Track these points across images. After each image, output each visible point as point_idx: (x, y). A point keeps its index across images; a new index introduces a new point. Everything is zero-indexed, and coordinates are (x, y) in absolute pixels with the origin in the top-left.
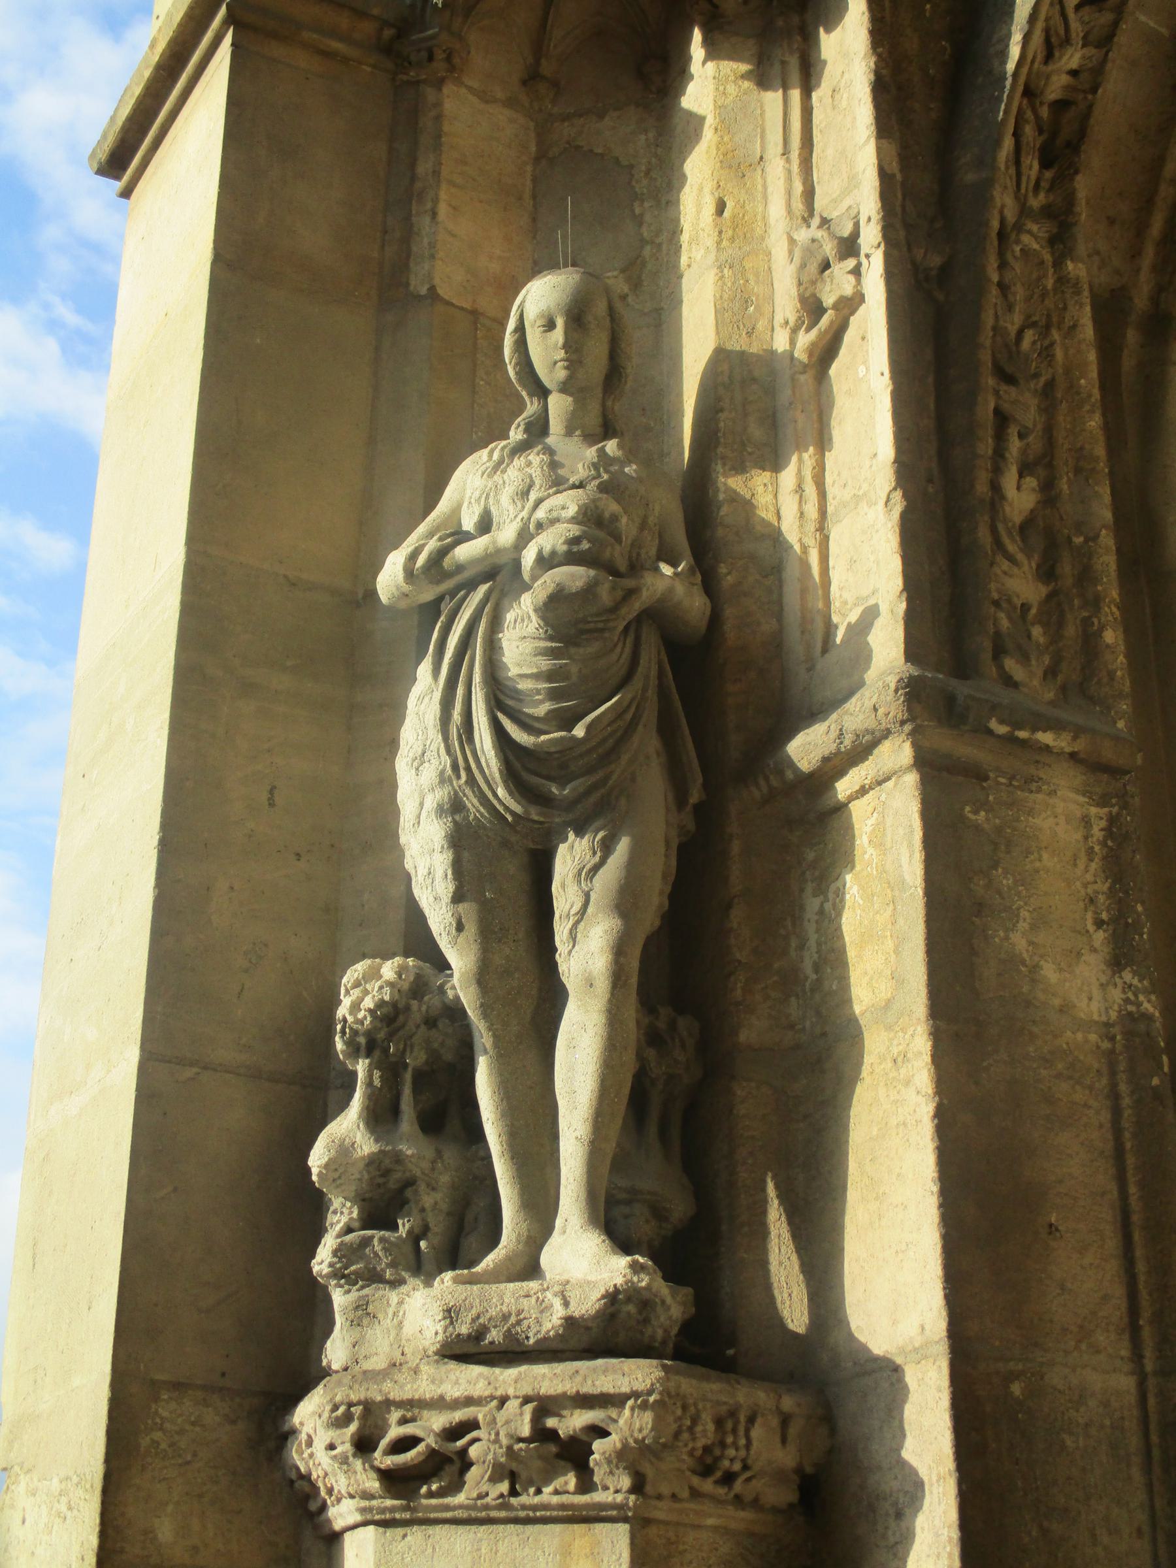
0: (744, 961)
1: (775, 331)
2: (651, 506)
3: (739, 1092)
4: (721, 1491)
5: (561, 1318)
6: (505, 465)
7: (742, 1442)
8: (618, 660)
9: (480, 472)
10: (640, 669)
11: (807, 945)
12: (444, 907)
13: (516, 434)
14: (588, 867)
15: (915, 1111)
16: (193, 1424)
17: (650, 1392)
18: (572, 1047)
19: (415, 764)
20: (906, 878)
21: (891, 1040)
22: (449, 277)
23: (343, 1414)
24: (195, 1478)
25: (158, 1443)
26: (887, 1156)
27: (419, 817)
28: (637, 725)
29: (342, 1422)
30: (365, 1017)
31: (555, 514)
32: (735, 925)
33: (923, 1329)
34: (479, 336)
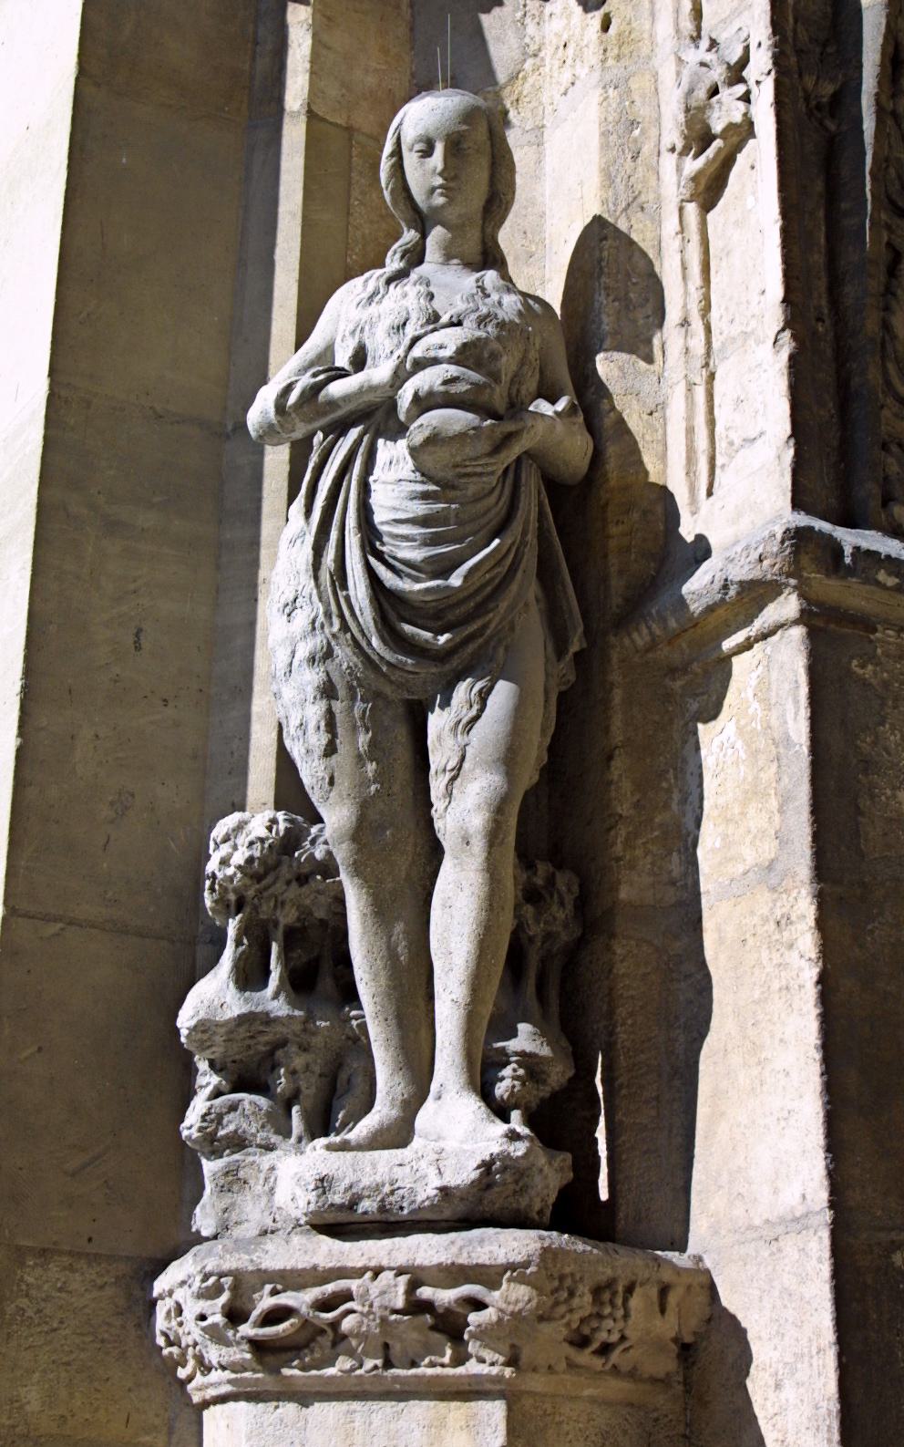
0: (624, 814)
1: (662, 156)
2: (531, 340)
3: (619, 951)
4: (598, 1362)
5: (437, 1188)
6: (380, 296)
7: (620, 1313)
8: (497, 503)
9: (355, 303)
10: (520, 513)
11: (690, 799)
12: (316, 761)
13: (393, 263)
14: (464, 721)
15: (798, 976)
16: (60, 1290)
17: (526, 1264)
18: (447, 906)
19: (287, 610)
20: (791, 734)
21: (775, 901)
22: (323, 92)
23: (213, 1284)
24: (62, 1345)
25: (23, 1309)
26: (769, 1020)
27: (291, 664)
28: (516, 571)
29: (210, 1293)
30: (235, 874)
31: (432, 354)
32: (615, 778)
33: (804, 1197)
34: (354, 154)
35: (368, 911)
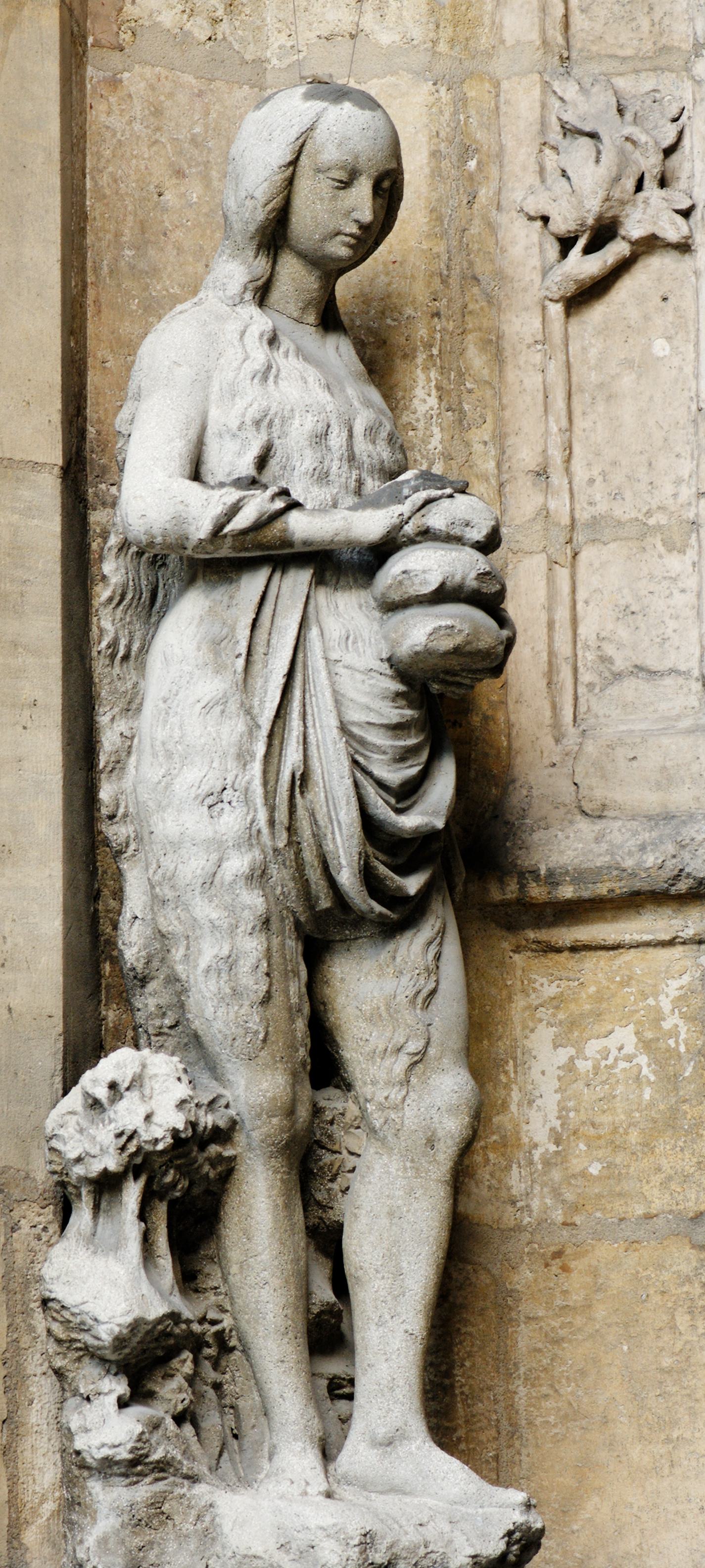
19: (210, 801)
35: (280, 1202)
